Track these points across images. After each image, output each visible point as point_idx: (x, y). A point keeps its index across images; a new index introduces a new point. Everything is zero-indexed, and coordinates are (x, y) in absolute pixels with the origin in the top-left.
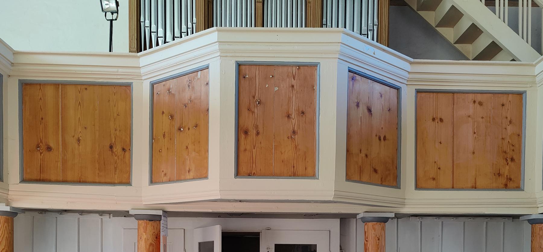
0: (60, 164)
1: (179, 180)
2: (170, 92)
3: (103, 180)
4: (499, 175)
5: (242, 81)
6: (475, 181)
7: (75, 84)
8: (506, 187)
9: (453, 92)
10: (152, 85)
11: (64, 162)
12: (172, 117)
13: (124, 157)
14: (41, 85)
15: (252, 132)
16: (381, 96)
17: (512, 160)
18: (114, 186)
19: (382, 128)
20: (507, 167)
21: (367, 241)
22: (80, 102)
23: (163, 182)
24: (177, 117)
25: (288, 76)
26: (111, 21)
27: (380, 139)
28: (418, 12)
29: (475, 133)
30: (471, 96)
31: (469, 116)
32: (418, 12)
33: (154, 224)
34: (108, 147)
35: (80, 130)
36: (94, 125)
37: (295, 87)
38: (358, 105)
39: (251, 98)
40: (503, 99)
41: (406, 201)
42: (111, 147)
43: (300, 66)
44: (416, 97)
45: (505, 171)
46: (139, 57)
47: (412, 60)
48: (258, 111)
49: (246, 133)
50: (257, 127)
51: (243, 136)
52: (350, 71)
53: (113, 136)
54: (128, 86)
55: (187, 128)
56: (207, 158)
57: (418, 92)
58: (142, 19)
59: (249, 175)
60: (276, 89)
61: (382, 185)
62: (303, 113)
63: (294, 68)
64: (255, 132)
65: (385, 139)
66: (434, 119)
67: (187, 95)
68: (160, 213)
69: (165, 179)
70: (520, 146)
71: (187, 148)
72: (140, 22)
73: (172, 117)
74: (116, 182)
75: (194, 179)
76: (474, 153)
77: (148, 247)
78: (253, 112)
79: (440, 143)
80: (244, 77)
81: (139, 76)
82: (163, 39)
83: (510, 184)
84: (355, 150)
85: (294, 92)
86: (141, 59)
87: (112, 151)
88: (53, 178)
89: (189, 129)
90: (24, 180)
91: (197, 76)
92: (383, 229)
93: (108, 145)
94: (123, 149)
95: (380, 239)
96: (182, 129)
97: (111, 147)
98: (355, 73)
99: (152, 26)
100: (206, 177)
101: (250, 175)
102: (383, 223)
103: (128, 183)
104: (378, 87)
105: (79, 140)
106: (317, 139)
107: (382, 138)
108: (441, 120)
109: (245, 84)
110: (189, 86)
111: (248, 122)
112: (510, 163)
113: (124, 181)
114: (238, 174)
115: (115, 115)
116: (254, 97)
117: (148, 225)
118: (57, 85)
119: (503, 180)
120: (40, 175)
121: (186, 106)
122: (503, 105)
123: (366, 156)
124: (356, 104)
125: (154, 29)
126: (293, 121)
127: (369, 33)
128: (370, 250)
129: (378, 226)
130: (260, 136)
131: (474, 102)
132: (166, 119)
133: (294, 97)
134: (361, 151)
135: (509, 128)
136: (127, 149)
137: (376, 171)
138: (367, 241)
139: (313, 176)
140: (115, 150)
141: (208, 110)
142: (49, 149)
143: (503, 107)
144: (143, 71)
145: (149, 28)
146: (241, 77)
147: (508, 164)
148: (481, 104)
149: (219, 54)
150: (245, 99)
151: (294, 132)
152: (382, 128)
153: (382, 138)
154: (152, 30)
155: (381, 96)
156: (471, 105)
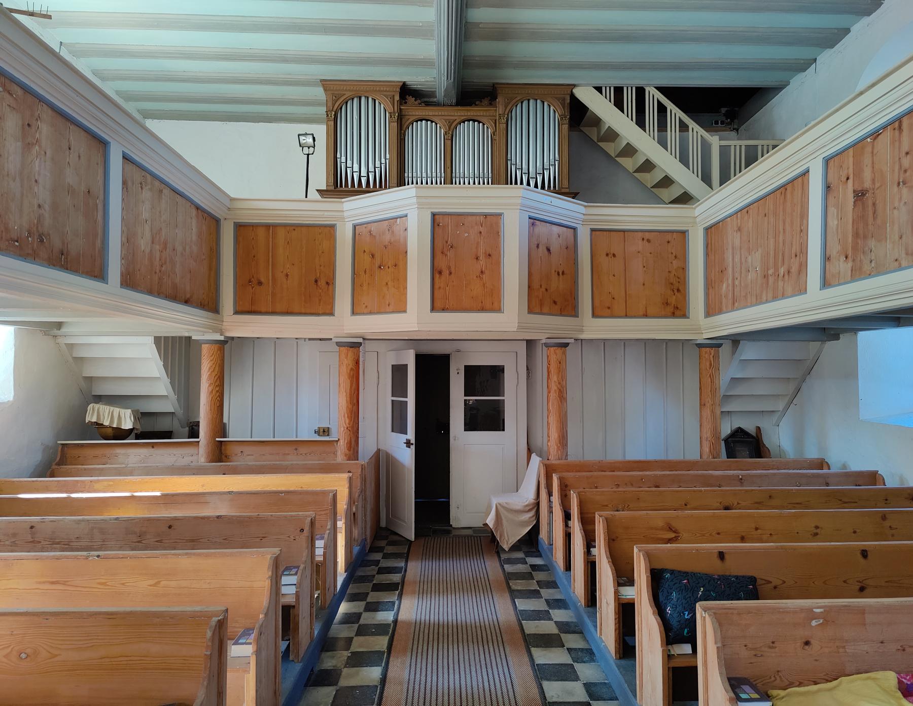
1: (379, 313)
2: (371, 234)
3: (308, 311)
5: (436, 227)
6: (646, 310)
7: (285, 226)
9: (624, 231)
10: (355, 227)
12: (373, 256)
13: (328, 289)
14: (254, 226)
15: (446, 272)
16: (559, 236)
18: (319, 316)
19: (560, 264)
20: (674, 297)
21: (549, 364)
22: (288, 242)
23: (364, 314)
24: (378, 256)
25: (476, 224)
26: (308, 155)
27: (558, 274)
28: (599, 143)
29: (644, 267)
30: (640, 234)
31: (639, 252)
32: (599, 143)
33: (355, 350)
35: (288, 266)
36: (301, 262)
37: (483, 233)
38: (538, 246)
39: (445, 243)
40: (669, 237)
41: (584, 328)
42: (316, 281)
43: (486, 216)
44: (591, 235)
46: (343, 202)
47: (586, 204)
48: (450, 254)
49: (440, 273)
50: (449, 268)
51: (437, 276)
52: (530, 218)
53: (318, 271)
54: (333, 227)
55: (387, 267)
56: (406, 294)
57: (593, 230)
58: (338, 156)
59: (443, 310)
60: (466, 235)
61: (561, 315)
62: (490, 255)
63: (482, 217)
64: (448, 272)
65: (563, 273)
66: (607, 255)
67: (387, 237)
68: (360, 340)
69: (365, 311)
71: (387, 284)
72: (337, 158)
73: (373, 256)
74: (320, 312)
75: (393, 312)
76: (644, 284)
77: (349, 372)
78: (446, 255)
79: (614, 275)
80: (438, 225)
81: (342, 219)
82: (358, 173)
85: (482, 238)
86: (345, 204)
87: (317, 284)
89: (389, 267)
91: (396, 222)
92: (564, 353)
94: (327, 283)
95: (561, 363)
96: (382, 267)
97: (316, 281)
98: (535, 219)
99: (348, 162)
100: (405, 311)
101: (444, 310)
102: (563, 348)
103: (331, 314)
104: (556, 229)
105: (287, 275)
106: (502, 276)
107: (561, 273)
108: (614, 255)
110: (389, 230)
111: (442, 263)
112: (676, 293)
113: (327, 312)
114: (433, 309)
115: (320, 252)
116: (447, 242)
117: (349, 352)
118: (267, 226)
120: (252, 308)
121: (386, 248)
122: (668, 242)
123: (546, 290)
124: (536, 246)
126: (481, 263)
127: (551, 167)
128: (552, 372)
129: (559, 351)
131: (643, 239)
132: (367, 258)
133: (482, 243)
134: (541, 286)
135: (674, 262)
136: (330, 283)
137: (555, 303)
138: (549, 364)
139: (499, 310)
140: (319, 283)
141: (406, 252)
143: (669, 244)
144: (346, 214)
145: (345, 164)
146: (436, 225)
147: (674, 294)
148: (649, 241)
149: (416, 206)
150: (439, 244)
151: (482, 272)
152: (560, 264)
153: (561, 273)
154: (348, 166)
155: (559, 236)
156: (640, 242)
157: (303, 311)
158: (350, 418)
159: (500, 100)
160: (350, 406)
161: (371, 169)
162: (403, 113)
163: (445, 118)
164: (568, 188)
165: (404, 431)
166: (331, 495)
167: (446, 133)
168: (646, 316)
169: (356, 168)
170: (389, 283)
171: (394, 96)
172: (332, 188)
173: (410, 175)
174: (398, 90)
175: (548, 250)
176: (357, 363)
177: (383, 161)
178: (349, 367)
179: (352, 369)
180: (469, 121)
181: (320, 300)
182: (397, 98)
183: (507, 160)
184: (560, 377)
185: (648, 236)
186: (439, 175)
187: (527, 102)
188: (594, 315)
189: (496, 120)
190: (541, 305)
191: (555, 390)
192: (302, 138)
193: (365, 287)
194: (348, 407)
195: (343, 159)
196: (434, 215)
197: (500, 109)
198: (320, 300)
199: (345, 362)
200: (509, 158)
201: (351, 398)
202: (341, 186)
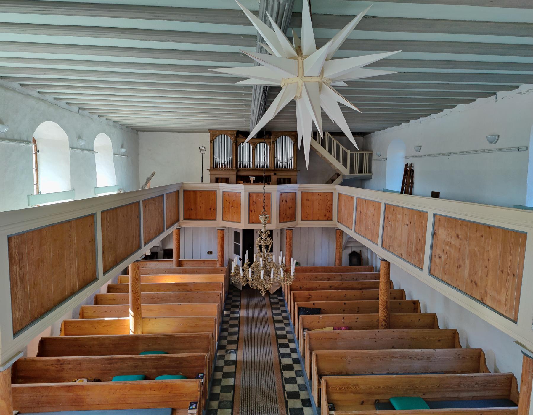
0: (195, 214)
2: (229, 196)
4: (326, 216)
7: (199, 191)
8: (328, 220)
9: (312, 192)
11: (196, 213)
12: (229, 203)
14: (189, 191)
15: (253, 211)
17: (330, 212)
30: (318, 193)
33: (223, 231)
34: (209, 209)
38: (283, 201)
42: (210, 209)
44: (301, 194)
45: (328, 215)
49: (251, 211)
50: (254, 210)
51: (250, 212)
54: (216, 191)
56: (240, 217)
57: (301, 192)
58: (214, 156)
61: (290, 221)
64: (254, 211)
70: (332, 207)
73: (229, 203)
81: (219, 189)
82: (221, 162)
83: (329, 219)
84: (282, 213)
88: (193, 218)
90: (185, 219)
93: (209, 208)
94: (214, 210)
97: (210, 209)
101: (253, 223)
103: (215, 220)
105: (201, 207)
108: (309, 200)
109: (251, 198)
111: (252, 208)
114: (249, 223)
118: (194, 191)
119: (326, 218)
123: (285, 214)
125: (218, 159)
129: (290, 231)
130: (255, 212)
132: (228, 203)
135: (329, 202)
136: (215, 209)
140: (211, 210)
142: (192, 210)
148: (320, 195)
150: (251, 202)
155: (290, 196)
157: (206, 218)
158: (221, 253)
159: (272, 136)
160: (222, 249)
161: (226, 161)
162: (238, 140)
163: (253, 142)
164: (296, 168)
165: (239, 255)
166: (222, 284)
167: (253, 148)
168: (319, 220)
169: (220, 160)
170: (235, 213)
171: (234, 135)
172: (212, 168)
173: (240, 162)
174: (236, 133)
175: (286, 201)
176: (224, 235)
177: (230, 158)
178: (221, 237)
179: (222, 237)
180: (261, 143)
181: (212, 215)
182: (235, 135)
183: (275, 158)
184: (290, 239)
185: (320, 194)
186: (250, 162)
187: (282, 136)
188: (302, 220)
189: (271, 143)
190: (284, 219)
191: (288, 244)
192: (200, 148)
193: (227, 212)
194: (221, 250)
195: (216, 157)
196: (249, 193)
197: (272, 140)
198: (212, 215)
199: (220, 235)
200: (275, 157)
201: (222, 247)
202: (215, 167)
